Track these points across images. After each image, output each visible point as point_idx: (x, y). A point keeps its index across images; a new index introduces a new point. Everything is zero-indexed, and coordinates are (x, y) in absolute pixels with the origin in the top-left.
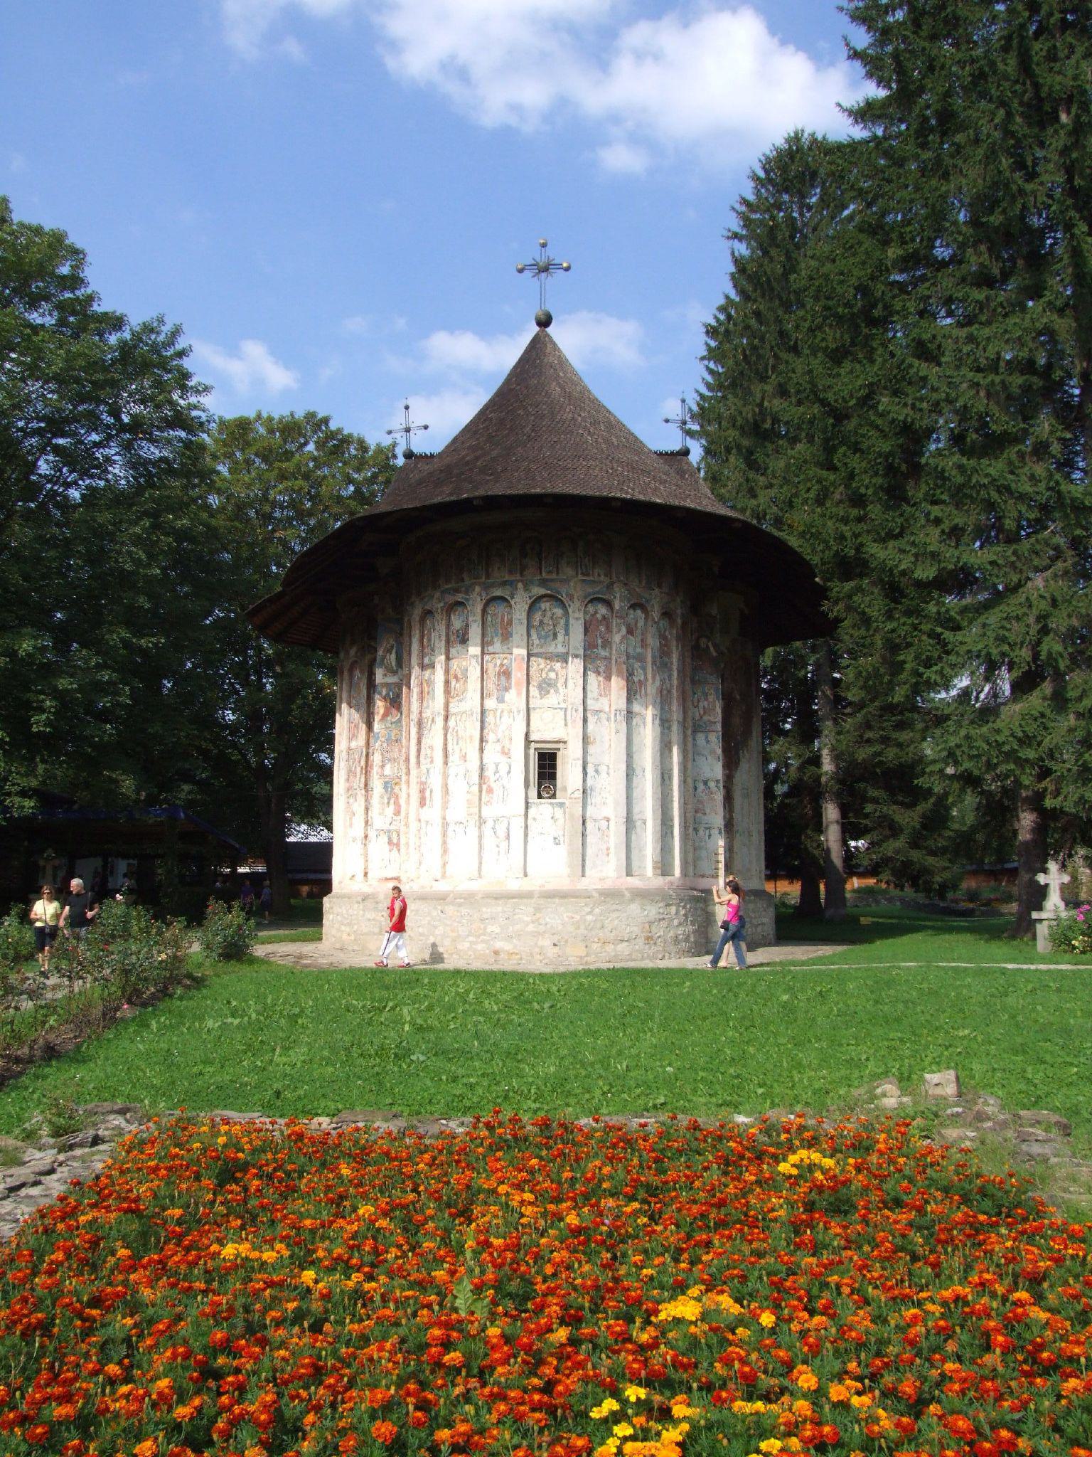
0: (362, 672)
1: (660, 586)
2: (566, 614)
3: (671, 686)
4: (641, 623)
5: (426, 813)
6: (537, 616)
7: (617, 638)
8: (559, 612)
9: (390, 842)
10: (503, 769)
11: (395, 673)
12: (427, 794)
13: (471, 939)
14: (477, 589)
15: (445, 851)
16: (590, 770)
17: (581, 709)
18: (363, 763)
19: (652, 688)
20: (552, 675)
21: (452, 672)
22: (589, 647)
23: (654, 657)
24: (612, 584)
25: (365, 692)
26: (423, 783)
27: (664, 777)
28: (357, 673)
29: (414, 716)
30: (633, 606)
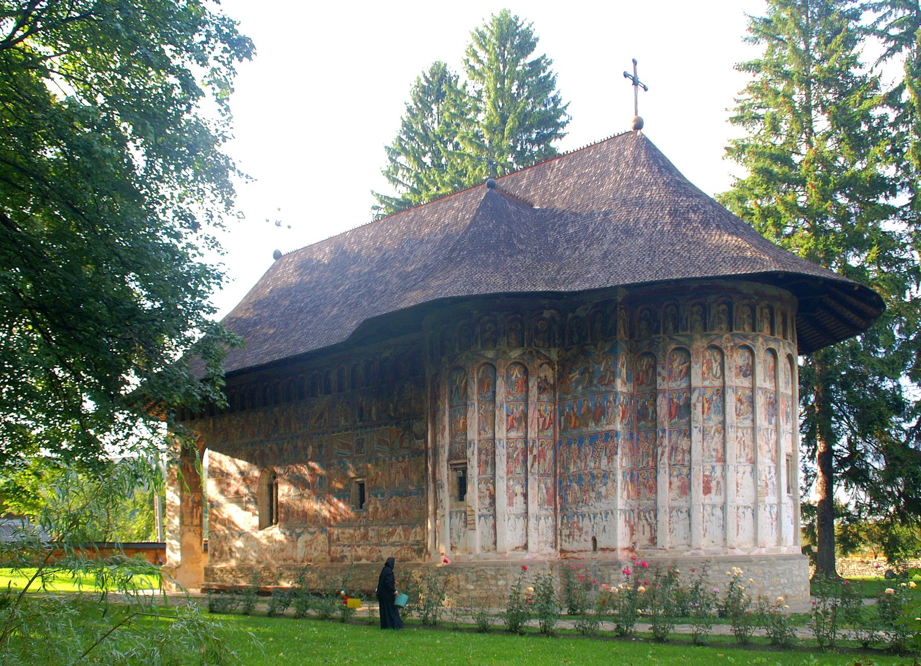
0: (526, 372)
5: (714, 498)
12: (713, 484)
15: (738, 526)
18: (535, 452)
25: (534, 392)
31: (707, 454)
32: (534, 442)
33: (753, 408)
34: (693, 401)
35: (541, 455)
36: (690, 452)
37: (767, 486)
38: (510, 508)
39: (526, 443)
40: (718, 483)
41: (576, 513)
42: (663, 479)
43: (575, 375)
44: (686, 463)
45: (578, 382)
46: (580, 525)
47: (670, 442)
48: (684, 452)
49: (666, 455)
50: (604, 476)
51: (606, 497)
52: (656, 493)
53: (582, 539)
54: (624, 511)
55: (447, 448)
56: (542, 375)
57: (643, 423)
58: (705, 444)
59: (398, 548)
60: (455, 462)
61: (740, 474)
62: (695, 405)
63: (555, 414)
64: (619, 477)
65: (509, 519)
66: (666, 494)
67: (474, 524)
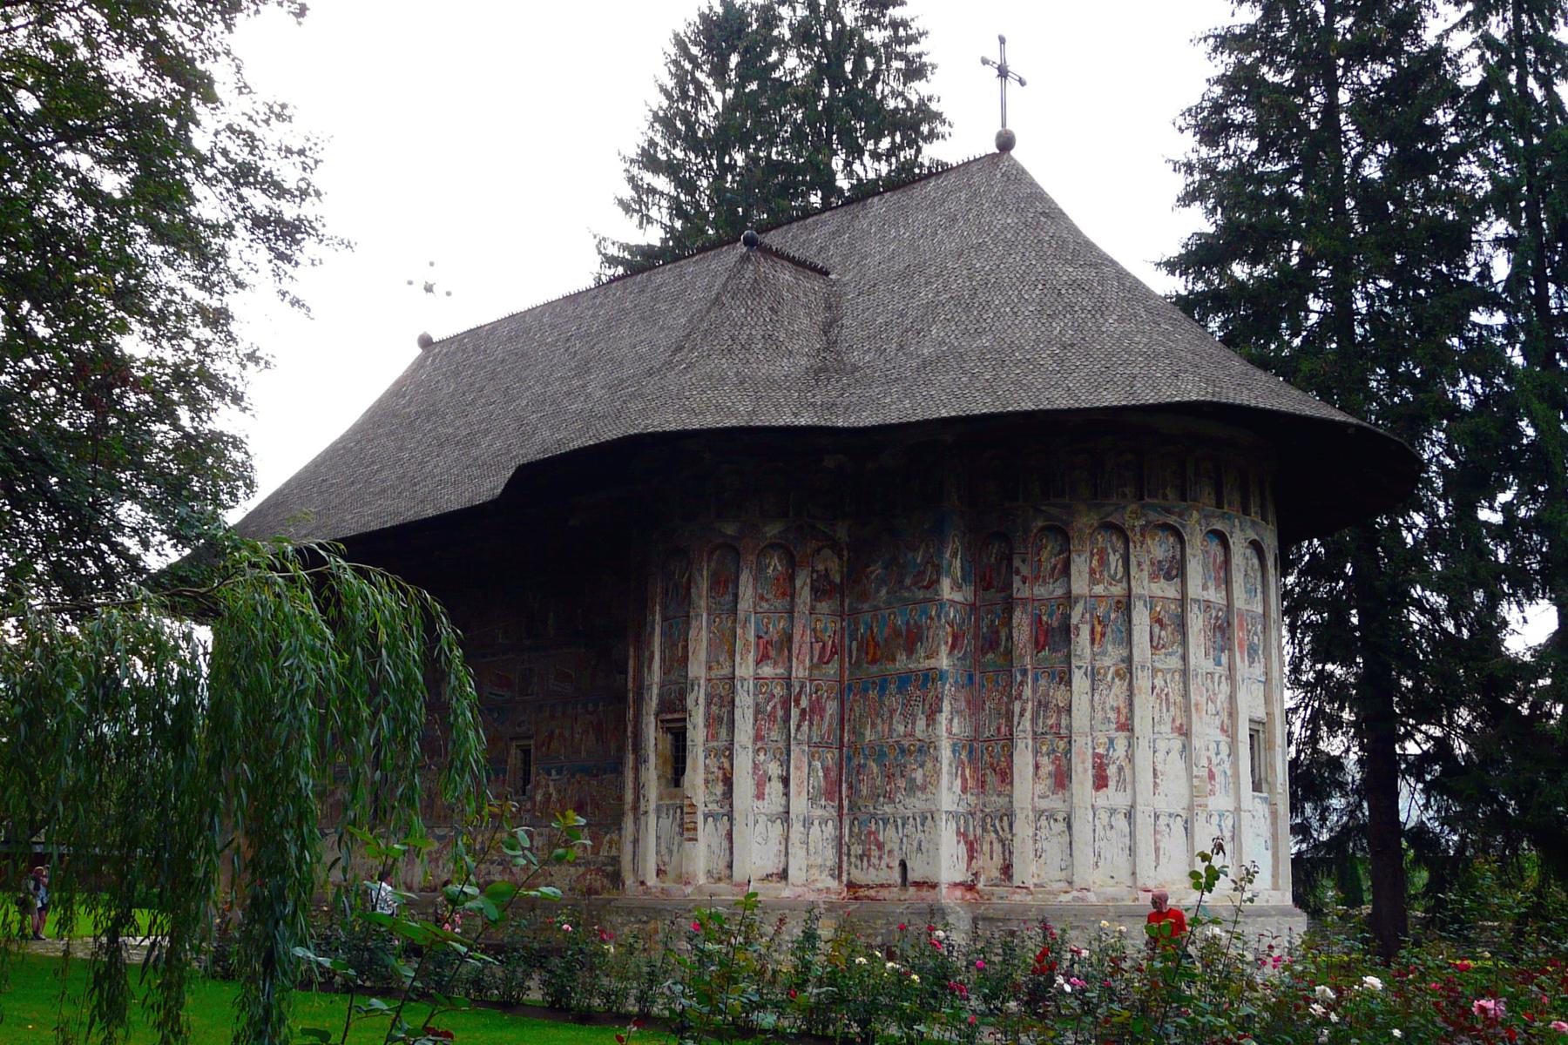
5: (1112, 797)
8: (1256, 561)
9: (958, 833)
10: (1224, 749)
11: (960, 588)
12: (1112, 771)
14: (1195, 515)
15: (1157, 850)
25: (805, 596)
26: (1100, 756)
31: (1099, 715)
32: (802, 686)
33: (1184, 635)
34: (1074, 620)
35: (816, 709)
36: (1069, 711)
37: (1212, 776)
38: (759, 803)
39: (789, 686)
40: (1120, 769)
41: (873, 816)
42: (1023, 760)
43: (877, 570)
44: (1063, 732)
45: (882, 582)
46: (881, 839)
47: (1034, 691)
48: (1059, 710)
49: (1028, 715)
50: (920, 750)
51: (923, 789)
52: (1011, 783)
53: (883, 864)
54: (955, 816)
55: (655, 691)
56: (821, 567)
57: (990, 656)
58: (1097, 697)
59: (582, 870)
60: (669, 717)
61: (1160, 755)
62: (1077, 628)
63: (842, 637)
64: (946, 753)
65: (756, 822)
66: (1027, 787)
67: (695, 829)
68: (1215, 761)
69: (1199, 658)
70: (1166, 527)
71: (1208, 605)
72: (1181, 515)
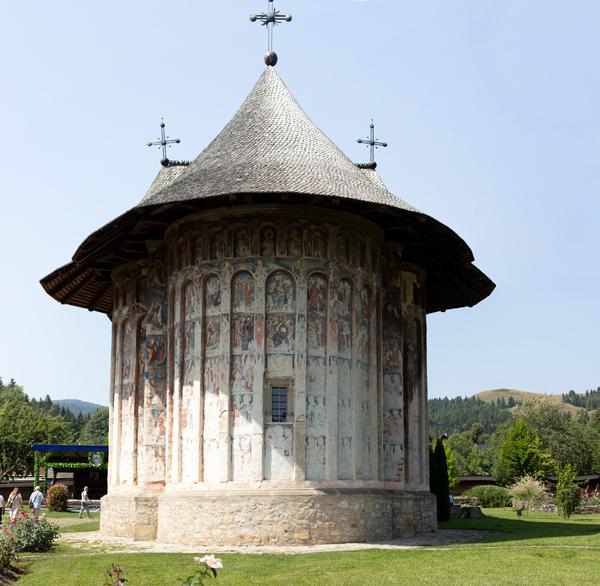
0: (132, 328)
1: (362, 265)
2: (294, 284)
3: (370, 339)
4: (348, 292)
6: (273, 285)
7: (331, 303)
8: (288, 282)
9: (156, 455)
10: (247, 399)
11: (160, 327)
12: (188, 419)
13: (223, 526)
14: (227, 264)
16: (311, 400)
17: (305, 355)
19: (356, 341)
20: (284, 330)
21: (208, 327)
22: (311, 309)
23: (357, 318)
24: (328, 262)
27: (365, 406)
28: (128, 327)
29: (177, 360)
30: (343, 280)
68: (239, 406)
69: (222, 347)
70: (213, 275)
71: (239, 315)
72: (219, 267)
